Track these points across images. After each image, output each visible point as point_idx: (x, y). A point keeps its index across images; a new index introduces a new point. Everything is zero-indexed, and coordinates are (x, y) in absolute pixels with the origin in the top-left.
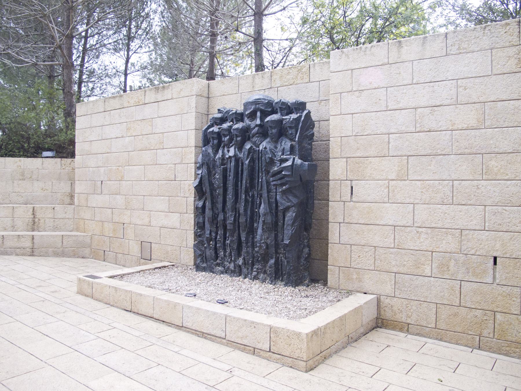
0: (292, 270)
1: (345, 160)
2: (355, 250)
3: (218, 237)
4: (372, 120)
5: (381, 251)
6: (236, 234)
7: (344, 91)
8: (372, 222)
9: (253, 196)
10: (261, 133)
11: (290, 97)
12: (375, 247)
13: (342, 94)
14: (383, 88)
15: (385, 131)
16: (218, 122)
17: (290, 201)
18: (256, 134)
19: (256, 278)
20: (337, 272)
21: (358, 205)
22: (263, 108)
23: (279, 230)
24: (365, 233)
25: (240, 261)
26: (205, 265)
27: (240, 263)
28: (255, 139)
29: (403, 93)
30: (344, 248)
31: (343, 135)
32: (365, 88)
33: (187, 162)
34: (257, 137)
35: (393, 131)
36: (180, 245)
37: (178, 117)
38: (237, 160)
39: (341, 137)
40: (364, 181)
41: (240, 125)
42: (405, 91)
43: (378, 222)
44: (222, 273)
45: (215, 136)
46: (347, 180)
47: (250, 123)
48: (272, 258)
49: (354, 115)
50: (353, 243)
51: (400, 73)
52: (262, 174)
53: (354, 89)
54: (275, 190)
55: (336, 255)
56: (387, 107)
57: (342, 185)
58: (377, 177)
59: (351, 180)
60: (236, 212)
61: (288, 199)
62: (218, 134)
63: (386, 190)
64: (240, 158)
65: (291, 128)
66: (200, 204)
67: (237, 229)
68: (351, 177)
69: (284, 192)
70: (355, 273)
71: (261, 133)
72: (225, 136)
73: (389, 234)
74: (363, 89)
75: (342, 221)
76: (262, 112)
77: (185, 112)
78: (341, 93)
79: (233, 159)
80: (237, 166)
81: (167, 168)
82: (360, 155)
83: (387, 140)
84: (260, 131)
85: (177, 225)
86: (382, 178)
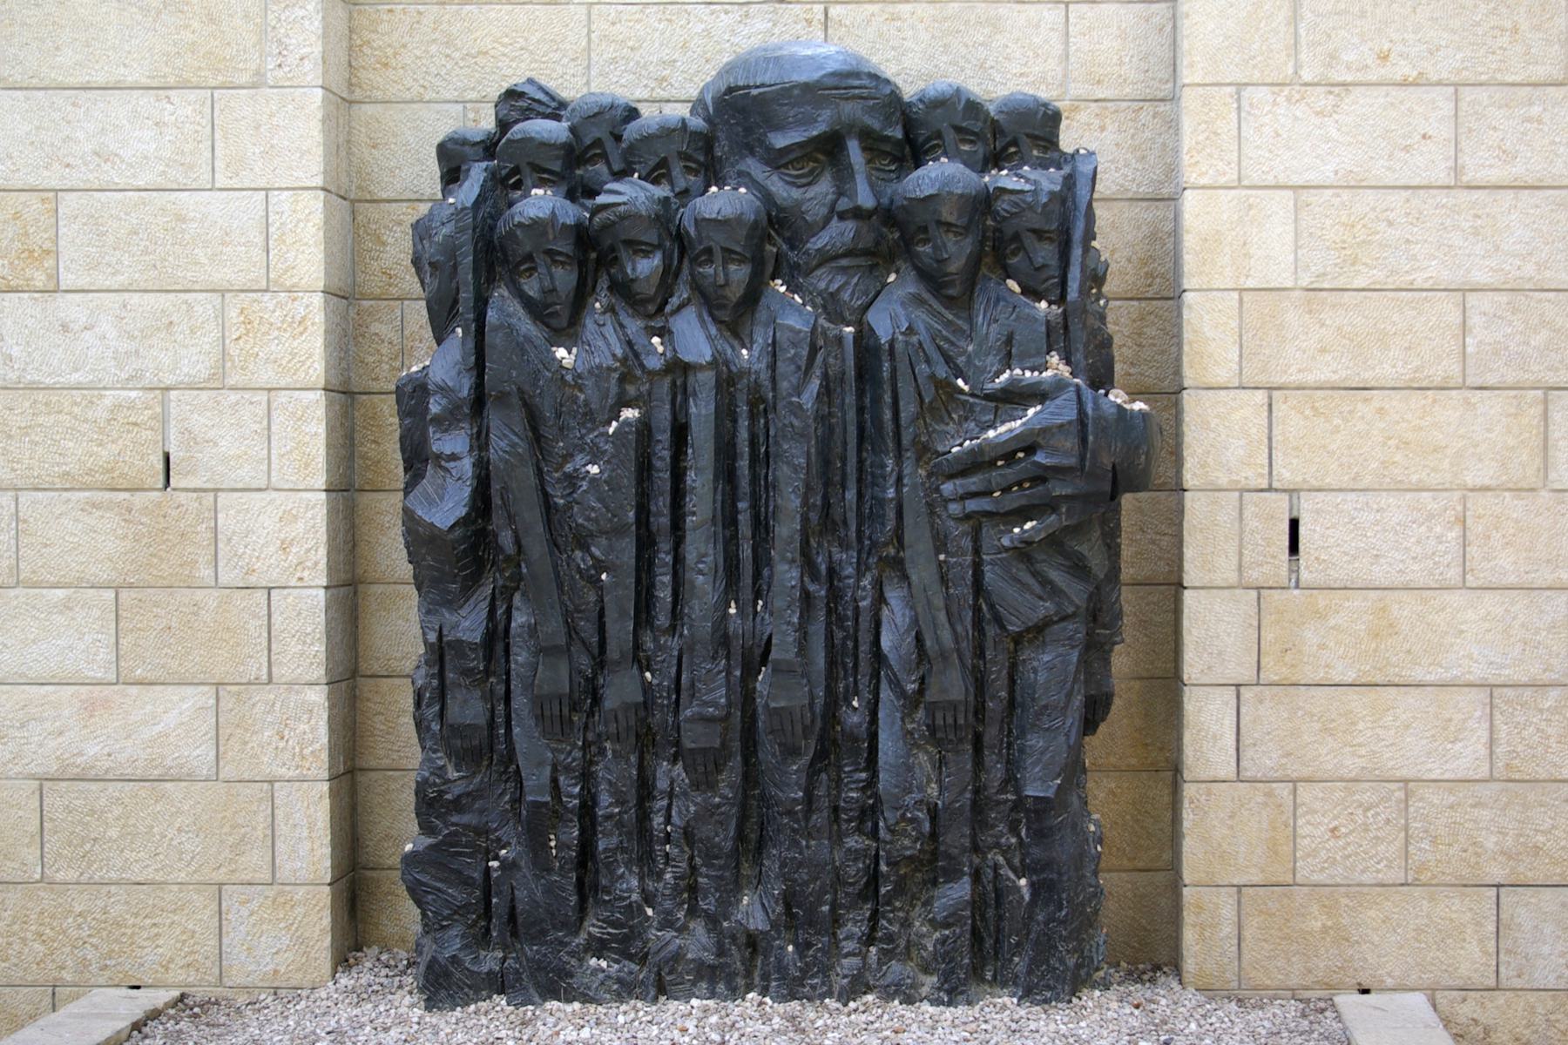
0: (1063, 922)
1: (1260, 396)
2: (1317, 805)
3: (605, 799)
4: (1390, 224)
5: (1434, 796)
6: (729, 779)
7: (1256, 77)
8: (1392, 675)
9: (832, 572)
10: (866, 253)
11: (999, 73)
12: (1406, 781)
13: (1247, 93)
14: (1439, 83)
15: (1446, 276)
16: (556, 166)
17: (1052, 590)
18: (849, 253)
19: (855, 989)
20: (1228, 911)
21: (1322, 599)
22: (875, 124)
23: (991, 733)
24: (1361, 726)
25: (751, 911)
26: (490, 960)
27: (758, 923)
28: (823, 280)
29: (1529, 120)
30: (1260, 799)
31: (1250, 284)
32: (1360, 77)
33: (266, 376)
34: (844, 270)
35: (1481, 277)
36: (220, 876)
37: (185, 107)
38: (727, 379)
39: (1241, 290)
40: (1352, 496)
41: (723, 201)
42: (1536, 110)
43: (1418, 674)
44: (626, 990)
45: (565, 246)
46: (1270, 489)
47: (796, 194)
48: (953, 875)
49: (1305, 195)
50: (1306, 772)
51: (1515, 30)
52: (899, 458)
53: (1307, 75)
54: (967, 543)
55: (1218, 835)
56: (1457, 170)
57: (1247, 514)
58: (1414, 478)
59: (1292, 492)
60: (728, 658)
61: (1045, 582)
62: (583, 236)
63: (1453, 534)
64: (744, 373)
65: (1039, 234)
66: (469, 624)
67: (736, 745)
68: (1286, 474)
69: (1024, 552)
70: (1315, 909)
71: (866, 253)
72: (639, 248)
73: (1470, 723)
74: (1349, 79)
75: (1248, 674)
76: (872, 143)
77: (244, 79)
78: (1240, 86)
79: (705, 381)
80: (725, 414)
81: (100, 413)
82: (1335, 377)
83: (1455, 317)
84: (867, 241)
85: (200, 755)
86: (1434, 480)
